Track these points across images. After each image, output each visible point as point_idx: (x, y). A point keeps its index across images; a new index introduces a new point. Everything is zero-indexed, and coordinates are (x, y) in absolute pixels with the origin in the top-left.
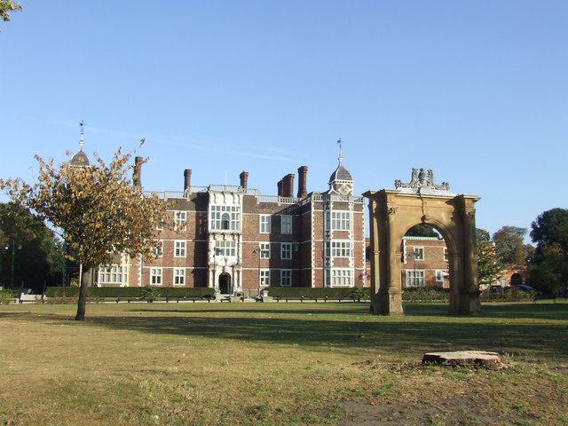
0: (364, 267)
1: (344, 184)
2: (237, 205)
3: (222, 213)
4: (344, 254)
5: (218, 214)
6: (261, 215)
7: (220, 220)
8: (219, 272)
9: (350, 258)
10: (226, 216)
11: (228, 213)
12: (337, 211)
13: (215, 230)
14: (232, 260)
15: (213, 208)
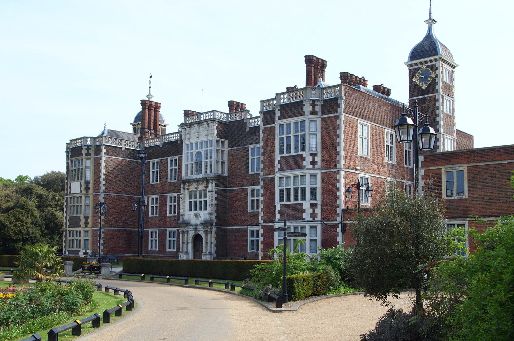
0: (339, 219)
1: (424, 66)
2: (210, 138)
3: (195, 151)
4: (296, 199)
5: (192, 153)
6: (250, 146)
7: (193, 162)
8: (192, 233)
9: (306, 205)
10: (199, 153)
11: (200, 150)
12: (285, 121)
13: (190, 177)
14: (204, 215)
15: (187, 145)
